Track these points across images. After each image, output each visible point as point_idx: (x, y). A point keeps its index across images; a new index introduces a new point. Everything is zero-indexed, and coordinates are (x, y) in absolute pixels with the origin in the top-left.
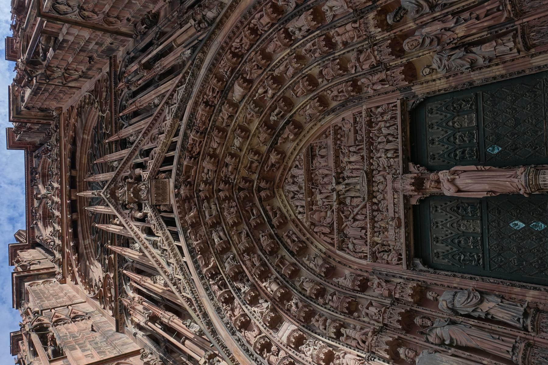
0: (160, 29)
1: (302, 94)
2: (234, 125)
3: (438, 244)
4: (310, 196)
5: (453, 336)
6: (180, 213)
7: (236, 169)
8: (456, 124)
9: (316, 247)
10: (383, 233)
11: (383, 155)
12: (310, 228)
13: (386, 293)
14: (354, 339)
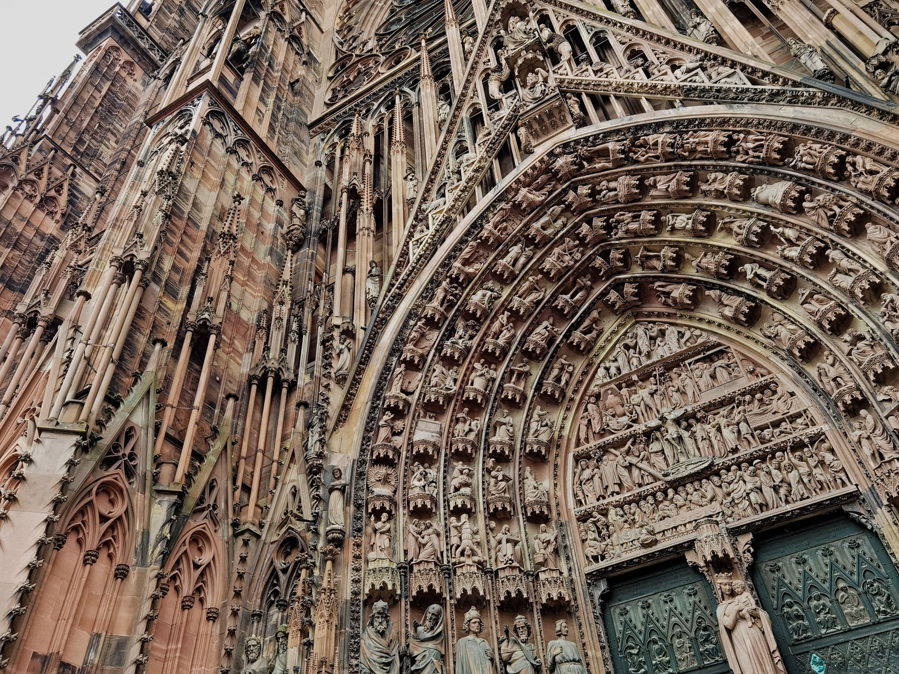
1: (811, 313)
2: (711, 206)
3: (639, 609)
4: (641, 377)
6: (525, 174)
7: (636, 234)
8: (842, 593)
9: (564, 419)
10: (626, 521)
11: (750, 486)
12: (590, 397)
13: (540, 559)
14: (460, 538)
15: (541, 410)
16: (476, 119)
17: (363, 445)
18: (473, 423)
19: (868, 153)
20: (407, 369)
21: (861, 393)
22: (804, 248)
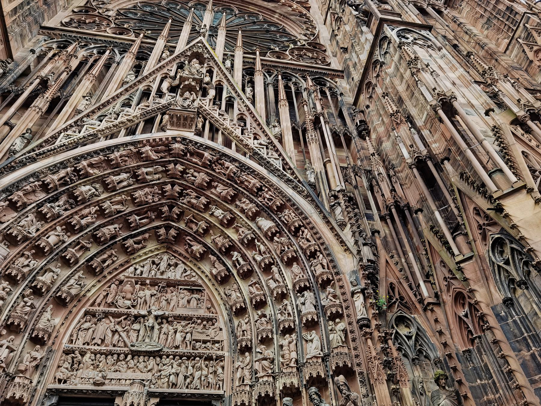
0: (354, 138)
1: (251, 293)
2: (236, 214)
4: (152, 283)
6: (154, 140)
7: (193, 206)
9: (94, 286)
10: (92, 365)
11: (174, 371)
12: (117, 280)
13: (22, 367)
15: (83, 274)
16: (146, 94)
18: (33, 262)
19: (312, 231)
20: (8, 206)
21: (251, 344)
22: (263, 260)
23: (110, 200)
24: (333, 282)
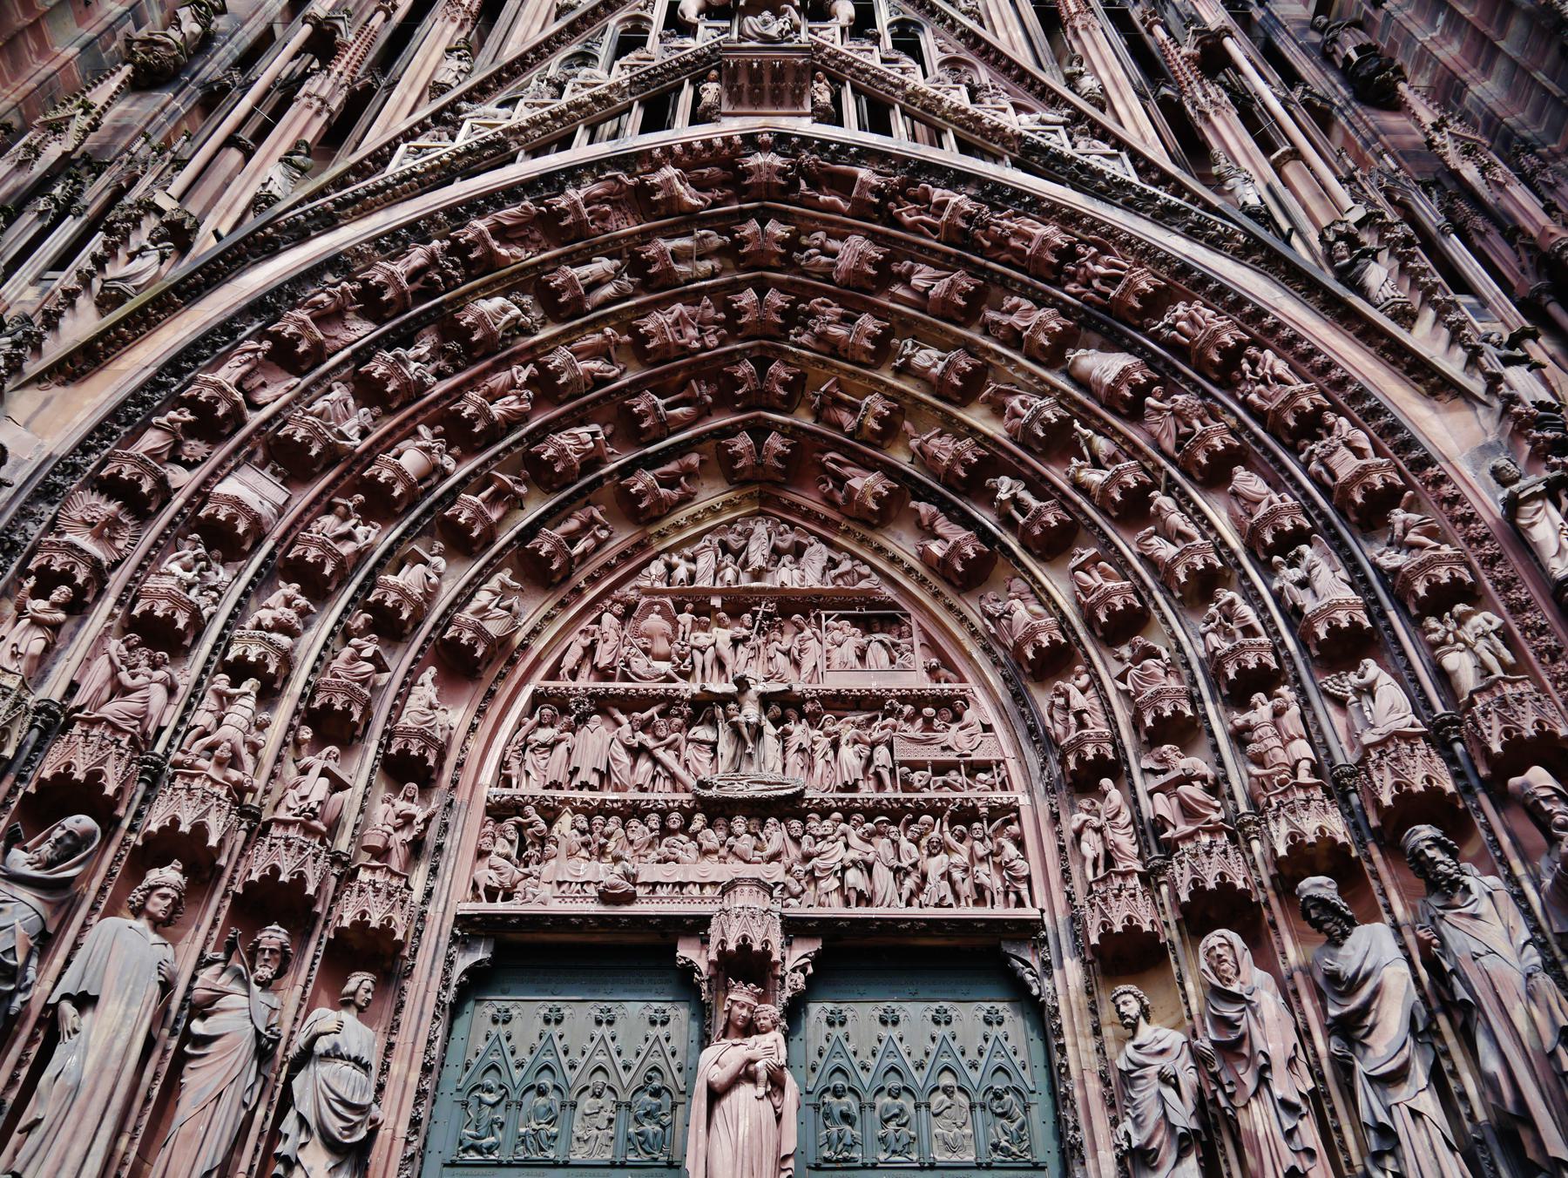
1: (1086, 590)
2: (988, 351)
5: (213, 1048)
6: (687, 147)
8: (942, 1097)
9: (548, 618)
10: (586, 845)
11: (853, 855)
17: (90, 436)
19: (1284, 352)
20: (269, 355)
23: (569, 344)
24: (1409, 493)
